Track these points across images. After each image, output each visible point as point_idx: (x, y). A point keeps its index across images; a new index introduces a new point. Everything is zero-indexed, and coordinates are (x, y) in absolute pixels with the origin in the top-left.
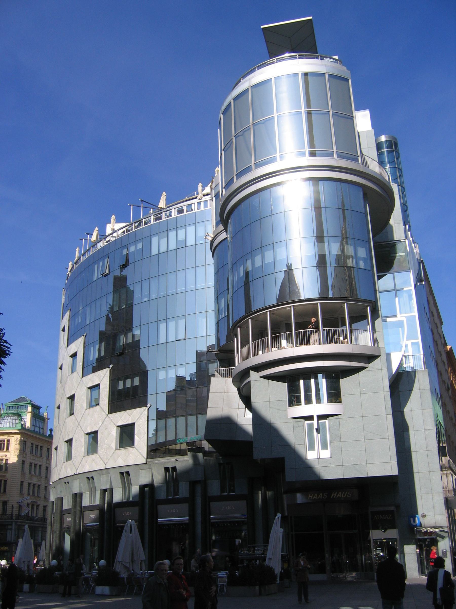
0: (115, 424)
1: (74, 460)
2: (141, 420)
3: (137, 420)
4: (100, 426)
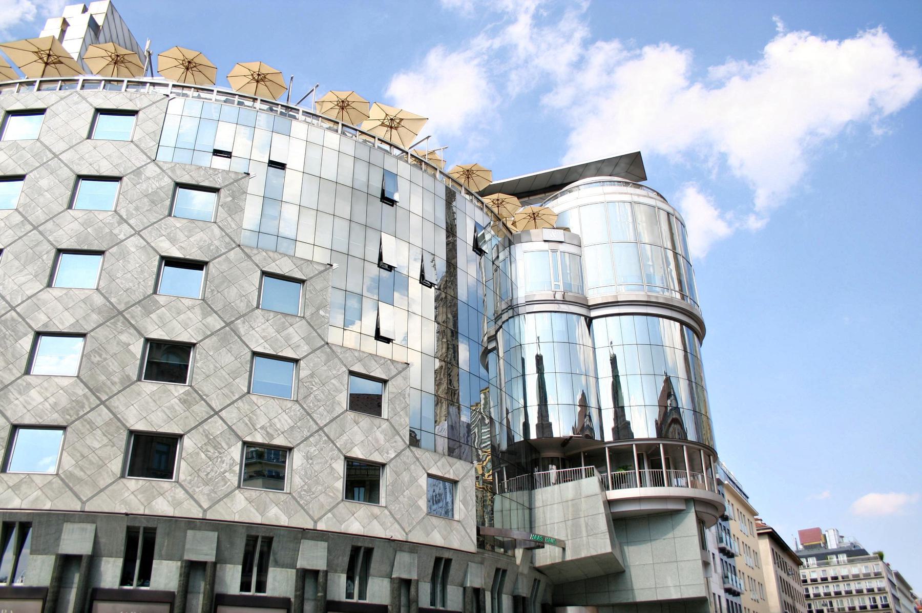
0: (424, 469)
1: (300, 497)
2: (468, 482)
3: (462, 478)
4: (392, 459)
